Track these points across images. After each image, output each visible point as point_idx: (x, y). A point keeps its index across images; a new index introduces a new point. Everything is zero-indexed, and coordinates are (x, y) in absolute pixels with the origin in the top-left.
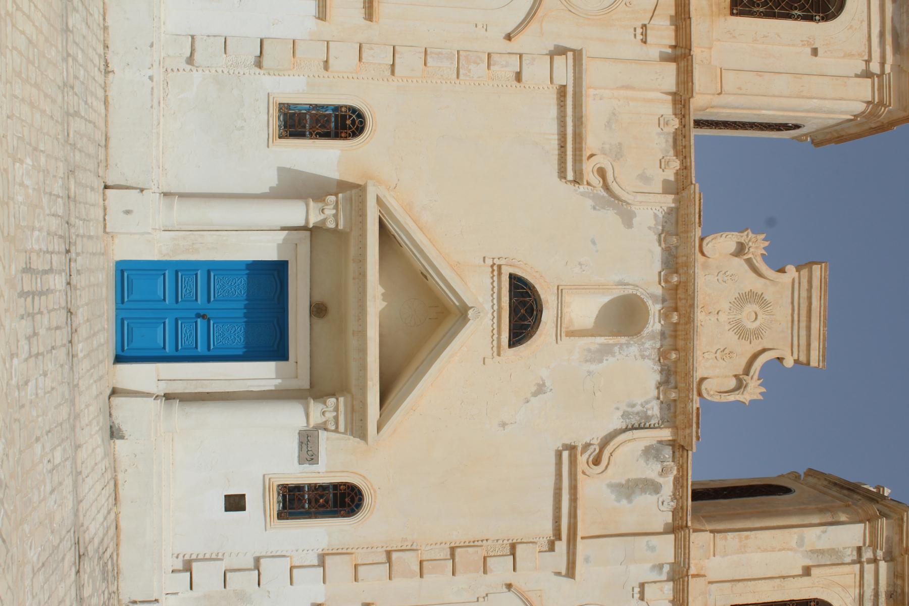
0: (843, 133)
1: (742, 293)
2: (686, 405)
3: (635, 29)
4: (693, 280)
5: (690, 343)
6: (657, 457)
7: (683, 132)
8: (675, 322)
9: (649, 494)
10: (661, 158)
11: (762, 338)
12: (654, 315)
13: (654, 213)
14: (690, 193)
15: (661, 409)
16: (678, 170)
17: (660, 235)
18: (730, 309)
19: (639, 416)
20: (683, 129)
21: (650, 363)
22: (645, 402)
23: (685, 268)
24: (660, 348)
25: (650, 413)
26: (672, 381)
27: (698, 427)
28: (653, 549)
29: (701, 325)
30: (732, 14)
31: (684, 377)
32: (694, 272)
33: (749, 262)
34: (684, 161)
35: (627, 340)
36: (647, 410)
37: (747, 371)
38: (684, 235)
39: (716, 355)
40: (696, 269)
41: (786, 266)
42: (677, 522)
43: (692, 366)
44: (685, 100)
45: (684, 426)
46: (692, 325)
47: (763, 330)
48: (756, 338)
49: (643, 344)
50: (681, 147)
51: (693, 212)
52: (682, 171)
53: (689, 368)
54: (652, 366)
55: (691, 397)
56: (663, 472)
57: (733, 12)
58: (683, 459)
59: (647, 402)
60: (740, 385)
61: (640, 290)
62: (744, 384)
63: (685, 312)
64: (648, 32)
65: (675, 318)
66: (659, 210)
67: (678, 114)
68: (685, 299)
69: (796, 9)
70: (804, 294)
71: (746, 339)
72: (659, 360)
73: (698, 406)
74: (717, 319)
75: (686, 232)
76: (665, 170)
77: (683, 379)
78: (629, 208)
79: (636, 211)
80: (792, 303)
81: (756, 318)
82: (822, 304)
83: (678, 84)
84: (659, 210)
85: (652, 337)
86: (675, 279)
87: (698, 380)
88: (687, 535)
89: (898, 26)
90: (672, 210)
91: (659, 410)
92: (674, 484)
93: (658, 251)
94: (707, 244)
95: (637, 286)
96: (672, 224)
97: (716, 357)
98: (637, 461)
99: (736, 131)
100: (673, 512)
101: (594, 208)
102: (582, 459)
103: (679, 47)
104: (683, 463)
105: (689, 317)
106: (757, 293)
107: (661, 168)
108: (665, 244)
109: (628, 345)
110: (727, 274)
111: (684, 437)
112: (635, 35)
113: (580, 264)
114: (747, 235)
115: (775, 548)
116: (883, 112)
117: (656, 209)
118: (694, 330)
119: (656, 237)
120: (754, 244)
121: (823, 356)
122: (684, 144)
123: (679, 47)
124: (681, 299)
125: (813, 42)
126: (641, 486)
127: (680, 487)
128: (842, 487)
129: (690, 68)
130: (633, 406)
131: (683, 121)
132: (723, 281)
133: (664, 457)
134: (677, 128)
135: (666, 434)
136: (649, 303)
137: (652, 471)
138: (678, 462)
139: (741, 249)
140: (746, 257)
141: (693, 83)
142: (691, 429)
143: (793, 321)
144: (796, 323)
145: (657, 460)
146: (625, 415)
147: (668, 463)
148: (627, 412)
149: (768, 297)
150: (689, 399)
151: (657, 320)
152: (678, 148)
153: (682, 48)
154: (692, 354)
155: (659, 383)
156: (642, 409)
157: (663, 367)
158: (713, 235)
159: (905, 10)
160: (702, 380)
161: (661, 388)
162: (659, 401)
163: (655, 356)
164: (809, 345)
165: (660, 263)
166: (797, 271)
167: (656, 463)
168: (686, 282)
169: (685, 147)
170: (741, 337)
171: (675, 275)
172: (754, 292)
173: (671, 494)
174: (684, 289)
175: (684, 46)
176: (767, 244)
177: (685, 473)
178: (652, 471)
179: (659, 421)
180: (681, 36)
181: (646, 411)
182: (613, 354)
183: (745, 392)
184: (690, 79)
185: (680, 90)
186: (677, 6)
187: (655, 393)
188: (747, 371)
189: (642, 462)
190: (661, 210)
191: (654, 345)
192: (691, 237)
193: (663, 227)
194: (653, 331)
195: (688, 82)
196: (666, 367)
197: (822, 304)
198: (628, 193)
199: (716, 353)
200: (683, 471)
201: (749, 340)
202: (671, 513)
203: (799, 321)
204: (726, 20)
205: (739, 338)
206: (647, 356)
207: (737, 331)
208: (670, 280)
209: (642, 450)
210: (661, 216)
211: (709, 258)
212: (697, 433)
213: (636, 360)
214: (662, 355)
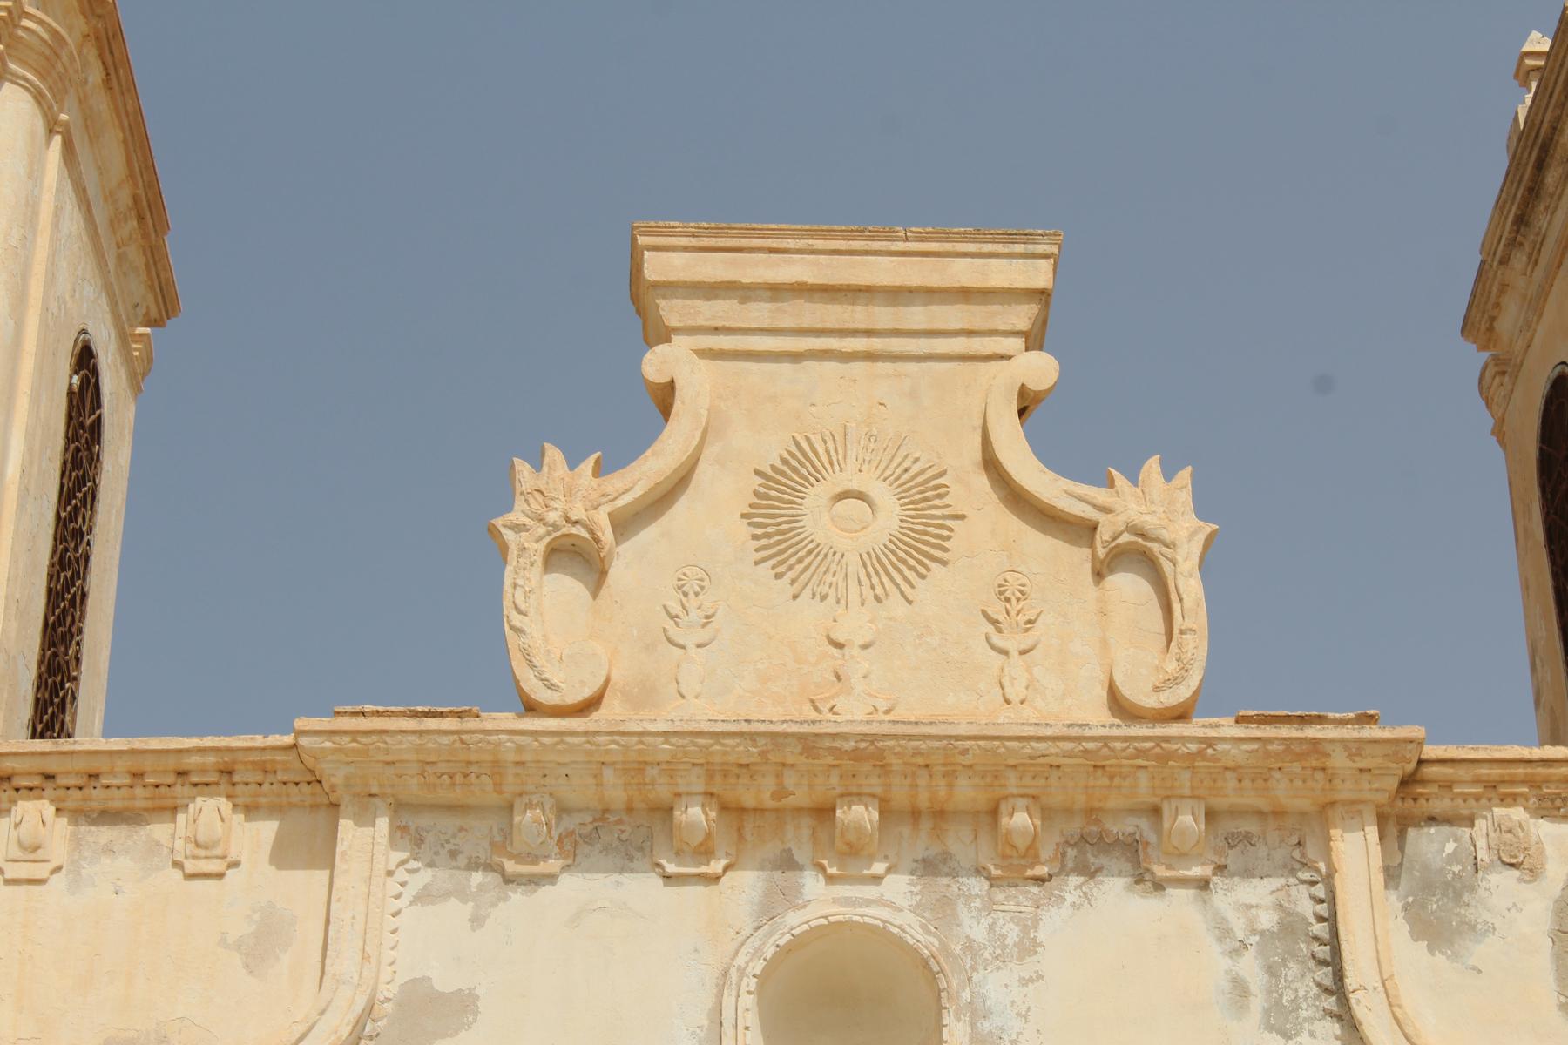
0: (125, 197)
2: (1226, 768)
4: (701, 741)
5: (965, 752)
6: (1459, 890)
7: (72, 781)
8: (876, 815)
10: (178, 874)
11: (942, 474)
12: (848, 902)
13: (411, 904)
14: (335, 750)
15: (1248, 873)
16: (235, 805)
17: (508, 880)
18: (824, 598)
20: (61, 781)
22: (1220, 940)
23: (652, 772)
24: (989, 878)
25: (1267, 919)
26: (1131, 829)
27: (1320, 720)
29: (888, 711)
31: (1111, 778)
32: (665, 734)
33: (627, 523)
34: (195, 779)
36: (1254, 932)
37: (1080, 530)
38: (510, 779)
39: (1014, 654)
40: (652, 728)
41: (646, 381)
43: (1060, 744)
45: (1319, 775)
46: (891, 743)
47: (906, 470)
48: (940, 496)
49: (970, 946)
50: (139, 791)
52: (240, 789)
53: (1070, 755)
54: (1066, 910)
55: (1193, 747)
59: (1223, 931)
61: (741, 960)
62: (1133, 538)
63: (835, 773)
66: (403, 884)
68: (779, 776)
70: (759, 313)
71: (945, 533)
72: (1040, 880)
73: (1231, 720)
74: (865, 647)
75: (497, 768)
76: (232, 857)
77: (1117, 781)
78: (388, 1007)
79: (401, 979)
80: (796, 357)
81: (861, 496)
82: (802, 244)
84: (403, 884)
85: (941, 912)
86: (695, 815)
90: (404, 829)
91: (1255, 881)
94: (551, 686)
95: (725, 973)
96: (461, 829)
97: (1023, 653)
99: (90, 602)
104: (1476, 781)
105: (856, 756)
106: (756, 493)
107: (220, 876)
108: (546, 857)
109: (977, 1012)
110: (676, 608)
111: (1366, 776)
114: (517, 528)
116: (41, 22)
117: (397, 897)
118: (910, 737)
119: (517, 896)
120: (552, 503)
121: (1011, 238)
122: (127, 781)
128: (1534, 191)
130: (1240, 989)
131: (24, 782)
132: (704, 625)
133: (1454, 858)
134: (53, 809)
136: (795, 922)
138: (1472, 802)
140: (607, 535)
142: (1328, 748)
143: (871, 357)
144: (876, 344)
145: (1472, 889)
147: (1481, 843)
148: (1267, 1012)
149: (771, 452)
150: (1200, 753)
151: (869, 891)
152: (140, 804)
155: (1139, 880)
156: (1252, 951)
157: (1070, 864)
160: (1118, 705)
161: (1161, 871)
162: (1215, 879)
163: (1021, 899)
164: (966, 294)
165: (626, 878)
167: (1481, 892)
168: (710, 771)
169: (138, 775)
171: (677, 813)
174: (738, 776)
176: (553, 454)
177: (1521, 771)
179: (1303, 882)
181: (1262, 933)
183: (1166, 535)
187: (1181, 896)
188: (1080, 530)
189: (1481, 951)
191: (977, 903)
192: (520, 749)
193: (473, 865)
194: (918, 905)
196: (1071, 852)
197: (802, 244)
198: (322, 1013)
199: (1005, 652)
201: (948, 523)
203: (869, 333)
205: (944, 563)
206: (1025, 930)
207: (911, 568)
208: (700, 838)
209: (1431, 949)
210: (426, 876)
211: (607, 681)
213: (1040, 977)
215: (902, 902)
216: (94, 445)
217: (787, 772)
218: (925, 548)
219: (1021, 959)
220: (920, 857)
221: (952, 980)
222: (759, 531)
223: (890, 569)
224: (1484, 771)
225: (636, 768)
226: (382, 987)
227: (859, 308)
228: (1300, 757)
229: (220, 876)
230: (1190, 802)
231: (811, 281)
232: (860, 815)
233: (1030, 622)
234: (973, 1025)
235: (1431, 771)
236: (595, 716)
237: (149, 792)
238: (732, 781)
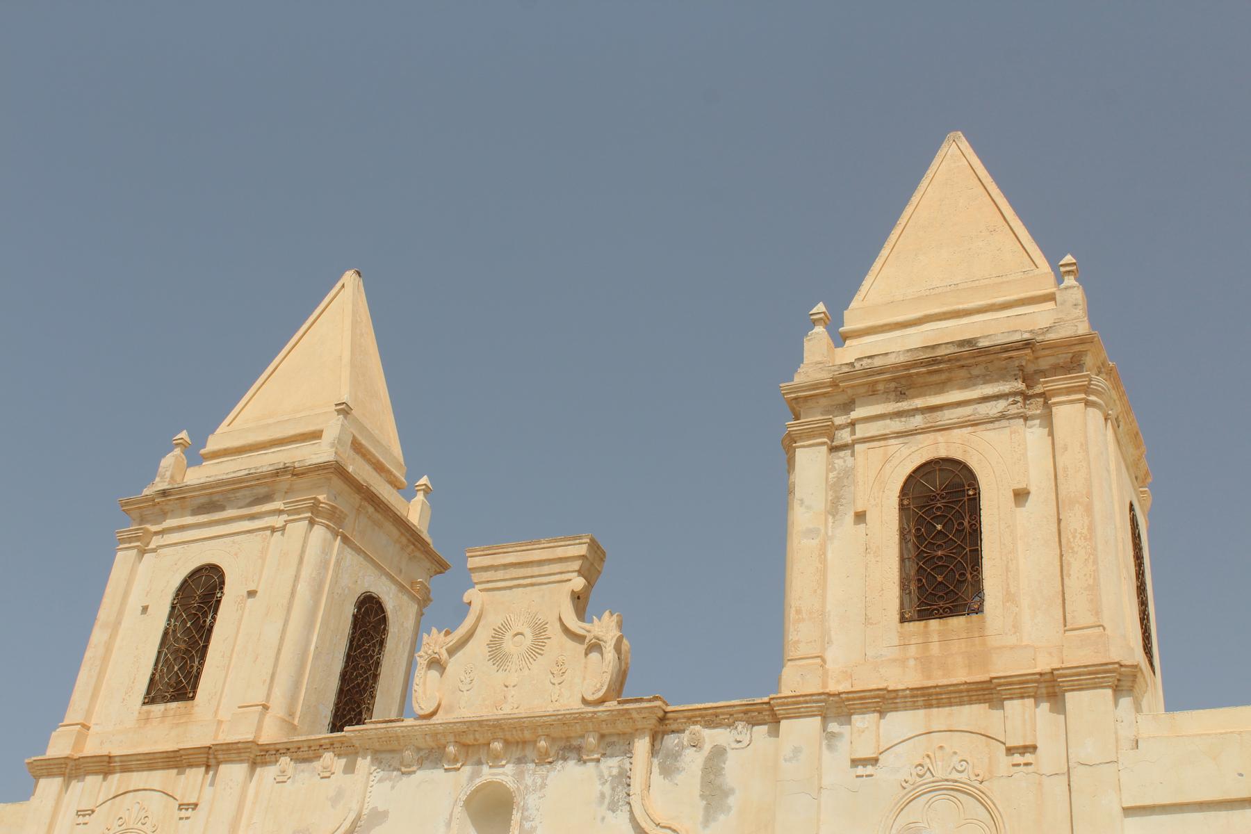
0: (404, 540)
2: (603, 721)
3: (181, 819)
4: (451, 725)
5: (524, 723)
6: (676, 756)
7: (293, 750)
8: (501, 745)
9: (725, 764)
11: (547, 623)
15: (612, 756)
16: (335, 755)
17: (403, 773)
21: (552, 775)
22: (600, 779)
23: (439, 736)
24: (536, 763)
25: (615, 772)
26: (579, 743)
28: (797, 751)
29: (517, 708)
30: (193, 698)
31: (569, 727)
32: (441, 724)
33: (452, 652)
34: (324, 747)
35: (517, 812)
36: (610, 776)
37: (578, 638)
39: (556, 684)
40: (437, 722)
42: (766, 717)
44: (261, 751)
45: (630, 720)
46: (503, 721)
48: (545, 631)
49: (526, 787)
50: (310, 752)
51: (374, 731)
52: (336, 750)
53: (554, 721)
55: (590, 715)
57: (192, 697)
58: (680, 718)
59: (601, 776)
60: (595, 647)
62: (596, 641)
63: (489, 732)
64: (186, 802)
65: (497, 746)
67: (276, 758)
68: (474, 734)
70: (500, 574)
71: (544, 644)
72: (550, 763)
73: (616, 703)
74: (514, 686)
79: (370, 807)
80: (510, 588)
83: (241, 761)
85: (519, 776)
86: (451, 749)
87: (583, 706)
88: (779, 701)
89: (248, 501)
90: (377, 759)
91: (614, 758)
92: (714, 727)
93: (421, 775)
94: (422, 709)
96: (393, 758)
97: (559, 684)
98: (677, 785)
100: (754, 725)
103: (207, 762)
104: (684, 717)
105: (494, 726)
107: (329, 777)
108: (413, 765)
109: (524, 809)
110: (463, 678)
111: (645, 720)
112: (187, 818)
114: (420, 657)
116: (326, 504)
118: (509, 719)
119: (405, 778)
121: (575, 539)
123: (207, 762)
124: (476, 740)
125: (241, 597)
126: (712, 777)
127: (761, 715)
129: (224, 747)
130: (603, 796)
133: (677, 745)
134: (289, 759)
135: (642, 745)
136: (477, 782)
137: (693, 761)
139: (436, 664)
140: (445, 655)
141: (239, 742)
142: (631, 711)
143: (532, 585)
144: (534, 580)
145: (680, 755)
146: (613, 808)
147: (685, 739)
151: (500, 770)
152: (311, 756)
153: (208, 758)
154: (537, 719)
155: (579, 761)
158: (413, 702)
159: (233, 496)
161: (585, 757)
163: (542, 770)
165: (434, 771)
166: (474, 587)
168: (456, 734)
169: (310, 747)
170: (540, 652)
172: (491, 641)
173: (728, 730)
175: (206, 756)
176: (434, 630)
177: (697, 713)
178: (693, 761)
180: (197, 760)
181: (612, 776)
183: (604, 638)
184: (235, 746)
185: (246, 758)
186: (169, 768)
187: (591, 765)
188: (578, 638)
189: (679, 778)
190: (375, 774)
191: (531, 772)
192: (402, 732)
194: (514, 774)
195: (238, 749)
196: (561, 752)
198: (344, 820)
200: (696, 717)
201: (545, 641)
202: (756, 728)
203: (532, 577)
204: (197, 705)
205: (542, 655)
206: (543, 781)
207: (532, 658)
208: (453, 757)
209: (664, 778)
211: (439, 706)
212: (650, 701)
213: (545, 796)
214: (544, 760)
215: (510, 773)
216: (381, 625)
217: (477, 733)
218: (537, 650)
219: (540, 790)
220: (517, 757)
221: (518, 799)
222: (491, 649)
223: (526, 659)
225: (435, 735)
226: (364, 810)
227: (529, 569)
228: (623, 715)
229: (329, 777)
230: (592, 733)
231: (514, 562)
232: (497, 746)
233: (563, 673)
234: (522, 813)
235: (669, 715)
236: (434, 718)
237: (313, 752)
238: (461, 737)
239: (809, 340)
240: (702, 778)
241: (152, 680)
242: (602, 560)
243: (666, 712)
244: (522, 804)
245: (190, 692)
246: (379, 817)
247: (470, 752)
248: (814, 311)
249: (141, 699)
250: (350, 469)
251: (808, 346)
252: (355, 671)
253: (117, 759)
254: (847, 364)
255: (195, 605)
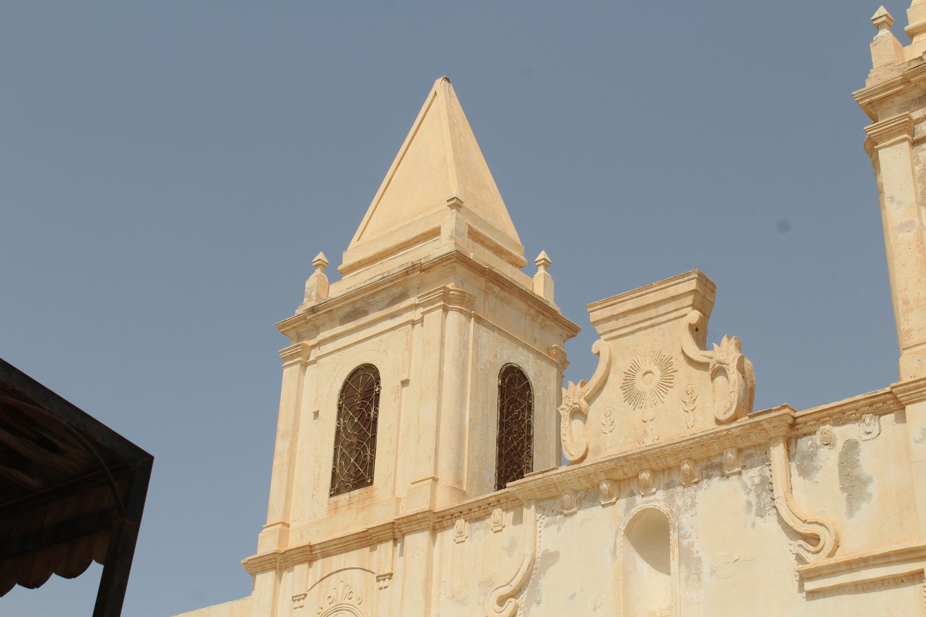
0: (533, 312)
1: (624, 397)
2: (737, 436)
3: (381, 589)
4: (600, 465)
5: (665, 450)
6: (811, 456)
8: (649, 475)
9: (859, 455)
10: (493, 532)
12: (647, 502)
14: (517, 490)
15: (752, 467)
16: (503, 510)
17: (566, 516)
18: (641, 407)
19: (762, 494)
21: (700, 493)
22: (744, 490)
24: (683, 486)
25: (757, 480)
26: (720, 461)
27: (770, 411)
29: (658, 439)
30: (371, 483)
31: (707, 448)
33: (590, 400)
34: (492, 505)
35: (674, 532)
36: (754, 485)
37: (703, 366)
38: (559, 487)
39: (690, 411)
40: (587, 464)
41: (596, 354)
42: (891, 406)
43: (689, 441)
44: (438, 518)
45: (763, 431)
47: (662, 360)
48: (671, 366)
49: (679, 509)
51: (533, 482)
54: (703, 490)
55: (725, 433)
56: (829, 443)
57: (370, 483)
59: (745, 487)
60: (720, 371)
63: (636, 464)
64: (382, 573)
65: (645, 476)
66: (541, 523)
67: (452, 522)
68: (623, 469)
69: (370, 414)
70: (621, 322)
71: (672, 377)
72: (696, 483)
73: (747, 418)
74: (651, 420)
75: (555, 485)
76: (503, 525)
77: (709, 448)
78: (539, 559)
79: (542, 551)
80: (633, 332)
81: (650, 372)
82: (629, 297)
83: (423, 530)
84: (541, 523)
85: (670, 500)
86: (605, 486)
87: (717, 426)
88: (900, 388)
89: (386, 302)
90: (540, 507)
92: (843, 424)
93: (581, 514)
94: (572, 455)
96: (554, 503)
97: (692, 410)
98: (817, 482)
100: (880, 415)
101: (539, 602)
102: (814, 561)
104: (814, 420)
105: (639, 458)
106: (625, 380)
107: (501, 530)
109: (680, 528)
110: (604, 422)
111: (776, 428)
112: (386, 587)
113: (595, 610)
114: (563, 409)
115: (918, 258)
116: (455, 291)
117: (540, 527)
118: (650, 450)
119: (568, 520)
120: (570, 400)
121: (684, 276)
122: (477, 509)
123: (394, 536)
124: (625, 474)
125: (396, 388)
126: (849, 470)
129: (405, 520)
130: (749, 504)
132: (611, 425)
133: (811, 446)
134: (464, 521)
135: (778, 452)
137: (828, 459)
138: (814, 426)
139: (578, 413)
140: (584, 404)
141: (417, 514)
142: (762, 423)
143: (652, 326)
145: (816, 455)
146: (761, 513)
150: (727, 434)
151: (652, 497)
152: (482, 514)
153: (394, 533)
154: (676, 445)
155: (722, 476)
156: (753, 492)
157: (704, 476)
158: (563, 451)
159: (372, 300)
161: (727, 472)
162: (743, 471)
163: (690, 491)
164: (674, 298)
166: (600, 339)
169: (480, 507)
170: (670, 385)
171: (600, 487)
172: (623, 384)
173: (857, 424)
174: (613, 472)
175: (391, 530)
176: (571, 384)
177: (824, 413)
178: (828, 459)
179: (767, 465)
180: (384, 535)
181: (756, 485)
182: (691, 545)
183: (727, 362)
184: (414, 518)
185: (426, 526)
186: (362, 547)
187: (734, 478)
188: (703, 366)
189: (818, 476)
190: (541, 520)
191: (680, 494)
192: (558, 479)
193: (557, 514)
195: (418, 519)
196: (704, 472)
197: (629, 297)
198: (521, 565)
199: (687, 412)
200: (824, 417)
202: (883, 418)
203: (651, 319)
204: (376, 489)
205: (672, 387)
206: (692, 500)
207: (663, 392)
208: (607, 493)
209: (804, 478)
210: (547, 519)
211: (587, 450)
212: (778, 410)
213: (696, 513)
214: (690, 481)
215: (661, 499)
216: (526, 392)
217: (624, 467)
218: (666, 384)
219: (691, 509)
220: (665, 483)
221: (672, 520)
222: (624, 391)
223: (658, 393)
224: (814, 416)
225: (588, 476)
226: (537, 554)
227: (647, 312)
228: (755, 428)
229: (501, 530)
230: (730, 449)
231: (632, 308)
232: (645, 476)
233: (694, 400)
234: (679, 533)
235: (799, 420)
236: (585, 461)
237: (484, 510)
238: (611, 474)
239: (875, 45)
240: (840, 472)
241: (334, 474)
242: (713, 291)
243: (795, 418)
244: (677, 524)
245: (368, 479)
246: (551, 557)
247: (622, 487)
248: (876, 15)
249: (327, 492)
250: (471, 256)
251: (874, 50)
252: (510, 435)
253: (317, 547)
254: (915, 59)
255: (359, 402)
